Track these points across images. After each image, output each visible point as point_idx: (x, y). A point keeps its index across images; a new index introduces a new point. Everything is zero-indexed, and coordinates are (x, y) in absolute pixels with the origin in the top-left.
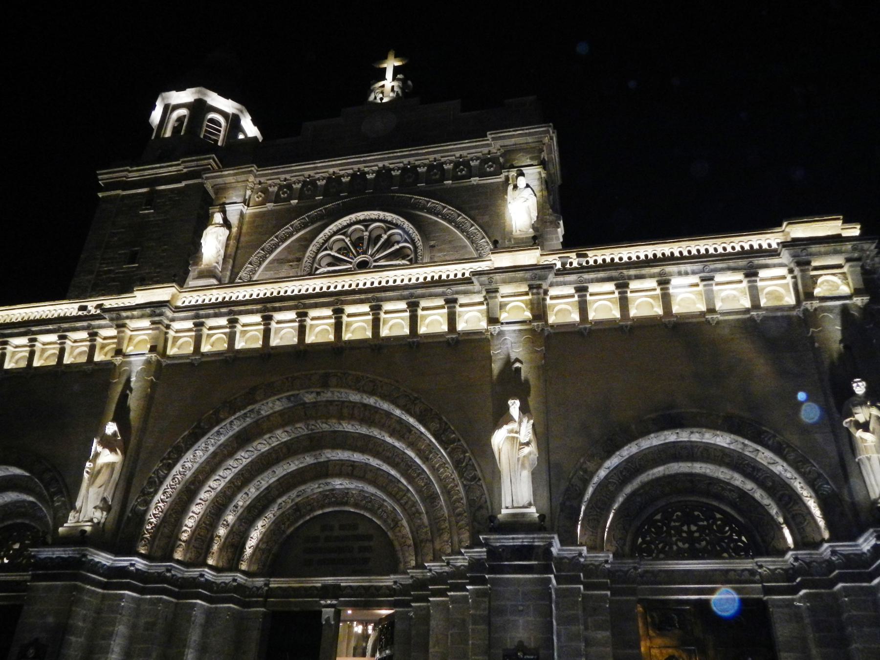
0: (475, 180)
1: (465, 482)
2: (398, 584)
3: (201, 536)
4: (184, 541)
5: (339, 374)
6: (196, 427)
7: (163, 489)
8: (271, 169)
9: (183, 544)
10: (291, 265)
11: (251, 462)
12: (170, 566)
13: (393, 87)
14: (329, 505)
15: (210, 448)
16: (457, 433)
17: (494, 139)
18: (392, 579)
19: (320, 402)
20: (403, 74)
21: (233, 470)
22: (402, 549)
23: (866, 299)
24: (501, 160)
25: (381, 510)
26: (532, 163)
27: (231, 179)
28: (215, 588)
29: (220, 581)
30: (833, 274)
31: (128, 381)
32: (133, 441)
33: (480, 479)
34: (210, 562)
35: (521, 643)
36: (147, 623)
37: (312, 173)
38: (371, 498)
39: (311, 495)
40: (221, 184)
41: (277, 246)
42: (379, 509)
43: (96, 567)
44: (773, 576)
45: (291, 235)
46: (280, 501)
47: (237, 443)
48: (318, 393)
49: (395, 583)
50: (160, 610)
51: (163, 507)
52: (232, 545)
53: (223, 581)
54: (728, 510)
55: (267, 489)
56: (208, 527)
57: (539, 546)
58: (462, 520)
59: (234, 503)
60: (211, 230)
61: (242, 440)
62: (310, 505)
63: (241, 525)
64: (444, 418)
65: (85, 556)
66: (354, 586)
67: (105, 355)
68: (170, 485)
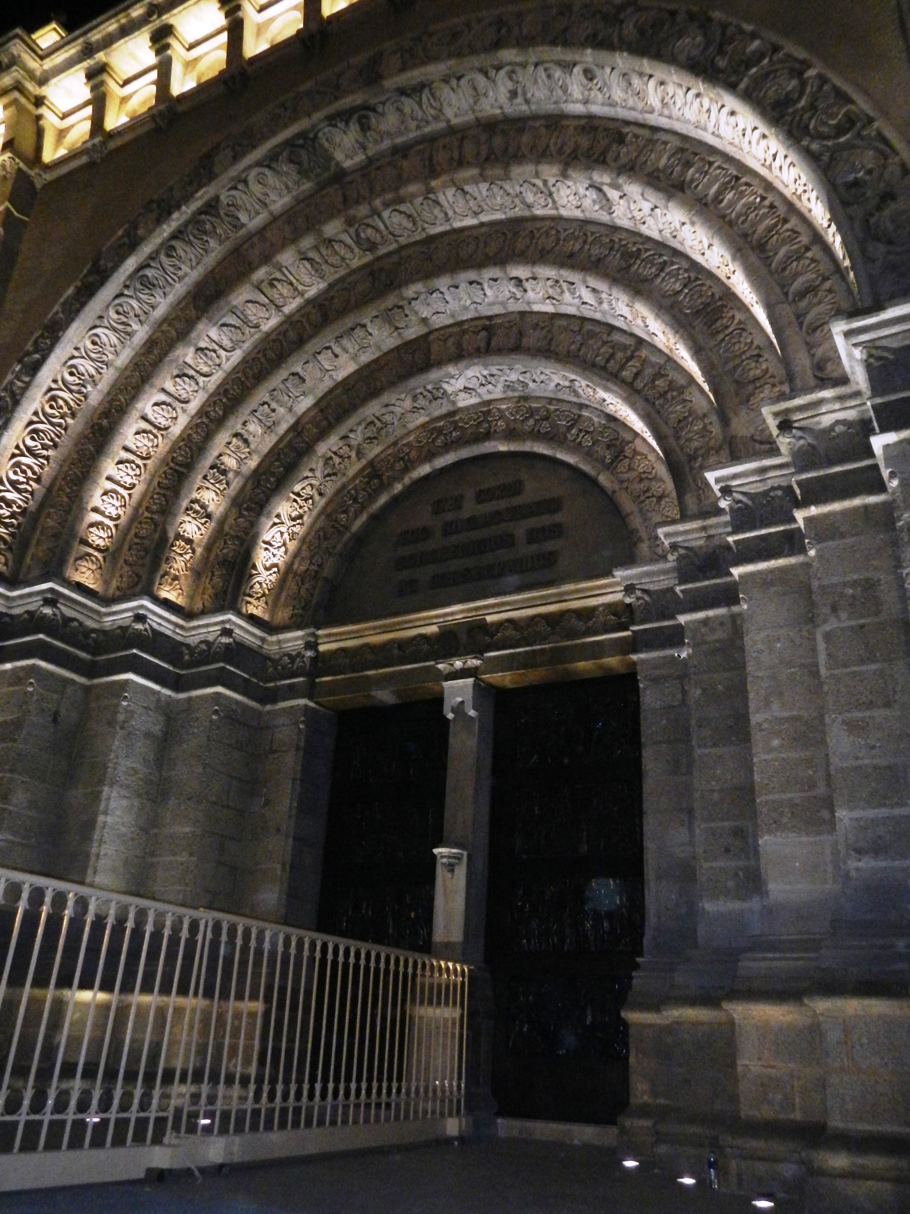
1: (815, 146)
3: (142, 538)
4: (97, 548)
6: (90, 272)
7: (26, 420)
9: (99, 556)
11: (244, 361)
12: (51, 590)
14: (448, 447)
15: (135, 327)
18: (618, 584)
19: (380, 156)
21: (201, 380)
22: (641, 511)
25: (574, 431)
28: (187, 657)
33: (871, 120)
34: (168, 593)
38: (548, 410)
39: (402, 438)
42: (569, 428)
46: (322, 448)
47: (195, 307)
49: (629, 589)
50: (31, 693)
51: (36, 469)
52: (224, 563)
53: (202, 638)
55: (293, 428)
56: (155, 517)
58: (819, 303)
62: (402, 459)
66: (521, 619)
68: (44, 414)
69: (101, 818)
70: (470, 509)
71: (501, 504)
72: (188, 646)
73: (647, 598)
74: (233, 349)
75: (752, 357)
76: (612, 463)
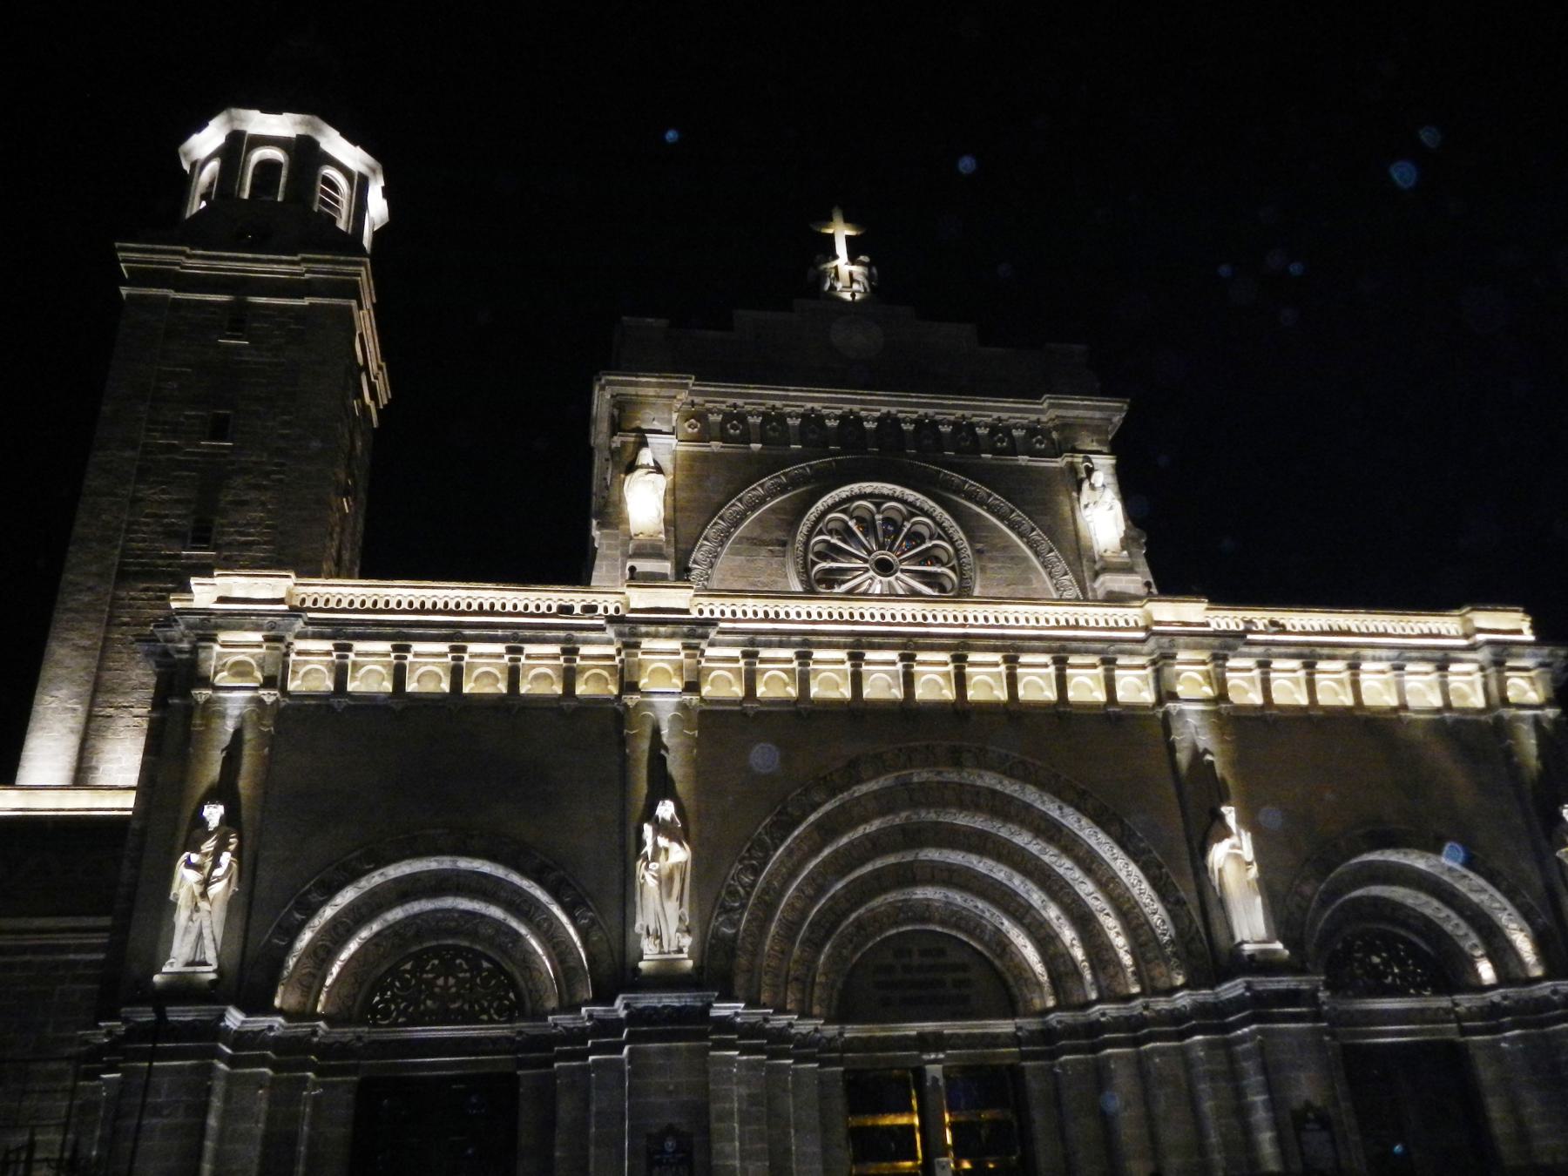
0: (1023, 460)
3: (772, 967)
8: (715, 386)
10: (770, 550)
13: (851, 274)
17: (1052, 406)
20: (870, 257)
23: (1558, 711)
24: (1055, 435)
26: (1099, 449)
27: (651, 391)
30: (1522, 677)
31: (656, 732)
32: (693, 829)
37: (778, 404)
40: (631, 395)
41: (744, 516)
42: (975, 928)
44: (1471, 1014)
45: (763, 501)
54: (1415, 939)
57: (1304, 991)
60: (640, 476)
61: (827, 830)
64: (1126, 821)
67: (586, 682)
70: (916, 960)
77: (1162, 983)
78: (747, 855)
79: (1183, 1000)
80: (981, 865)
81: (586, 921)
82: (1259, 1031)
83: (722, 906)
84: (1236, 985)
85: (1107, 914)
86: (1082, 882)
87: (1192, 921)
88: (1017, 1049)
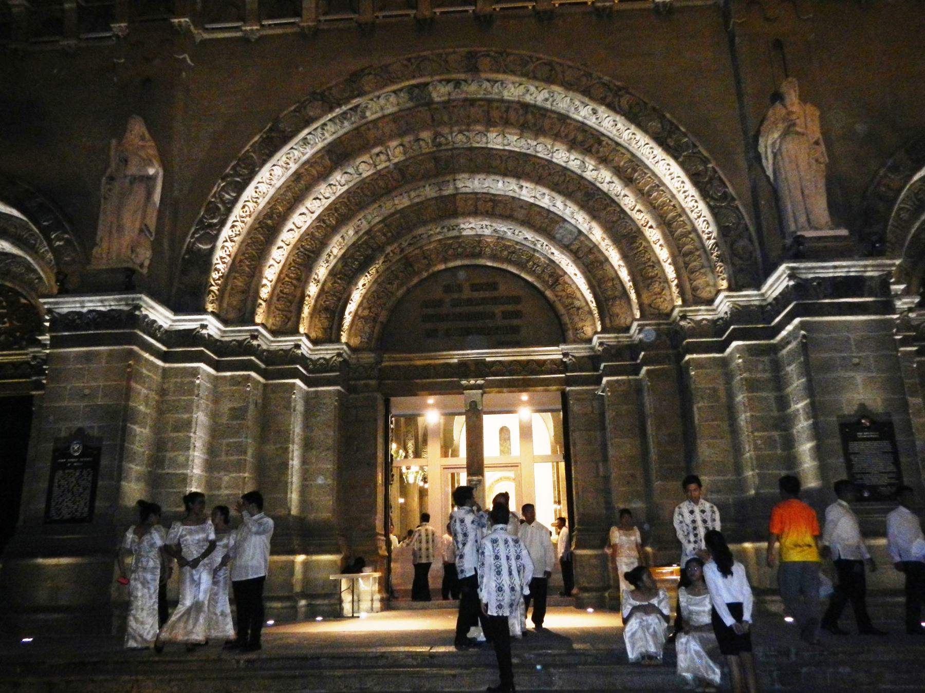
1: (712, 203)
2: (570, 357)
3: (286, 294)
5: (492, 54)
6: (271, 129)
11: (347, 191)
14: (456, 256)
16: (689, 135)
21: (324, 201)
22: (568, 313)
25: (531, 263)
28: (311, 366)
29: (317, 357)
33: (733, 199)
35: (862, 406)
36: (231, 409)
38: (515, 248)
42: (528, 261)
43: (151, 327)
47: (330, 159)
48: (458, 84)
49: (565, 355)
50: (249, 391)
52: (326, 309)
53: (322, 356)
56: (294, 282)
57: (871, 277)
58: (695, 261)
59: (328, 251)
63: (335, 282)
64: (668, 116)
65: (138, 307)
69: (291, 462)
70: (466, 294)
71: (487, 294)
72: (311, 360)
73: (574, 359)
74: (344, 185)
75: (650, 266)
76: (552, 285)
77: (705, 294)
78: (231, 172)
79: (723, 305)
80: (524, 191)
81: (61, 243)
82: (802, 325)
83: (201, 222)
84: (779, 277)
85: (651, 227)
86: (625, 196)
87: (740, 218)
88: (563, 375)
